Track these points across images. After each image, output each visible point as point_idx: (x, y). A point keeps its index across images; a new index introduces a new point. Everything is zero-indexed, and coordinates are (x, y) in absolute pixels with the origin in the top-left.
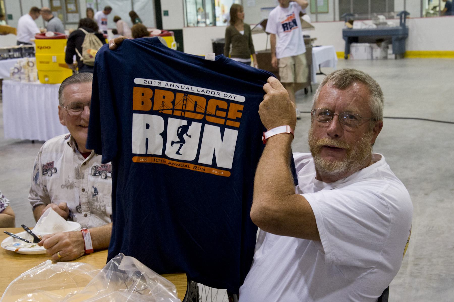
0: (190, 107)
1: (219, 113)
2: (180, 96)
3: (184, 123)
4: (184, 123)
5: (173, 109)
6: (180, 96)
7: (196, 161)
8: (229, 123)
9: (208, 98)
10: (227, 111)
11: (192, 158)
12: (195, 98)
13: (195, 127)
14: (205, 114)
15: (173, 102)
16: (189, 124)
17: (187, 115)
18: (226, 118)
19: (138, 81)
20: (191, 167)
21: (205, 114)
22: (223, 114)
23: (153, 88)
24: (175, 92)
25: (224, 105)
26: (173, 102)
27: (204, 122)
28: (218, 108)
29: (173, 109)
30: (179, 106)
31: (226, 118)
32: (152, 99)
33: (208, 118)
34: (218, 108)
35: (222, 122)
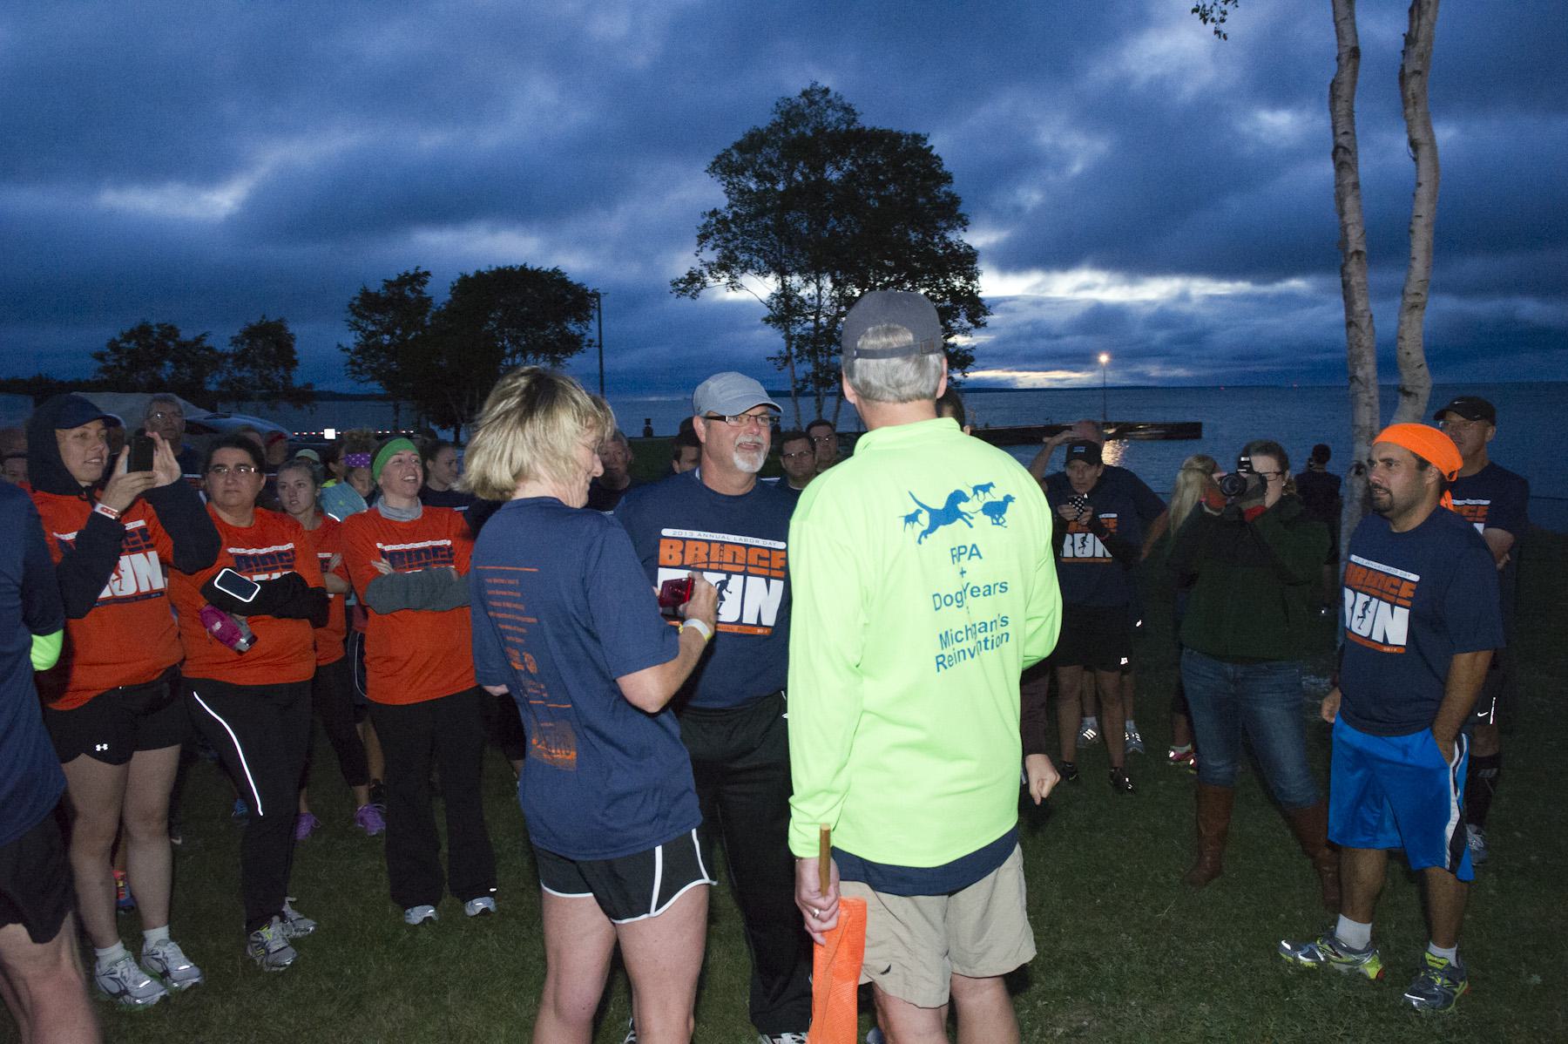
0: (728, 557)
1: (762, 563)
2: (715, 547)
3: (723, 577)
4: (723, 577)
5: (709, 562)
6: (715, 547)
7: (739, 622)
8: (774, 573)
9: (747, 546)
10: (769, 559)
11: (735, 618)
12: (736, 548)
13: (736, 582)
14: (746, 565)
15: (708, 554)
16: (729, 577)
17: (727, 567)
18: (770, 568)
19: (666, 532)
20: (735, 629)
21: (746, 565)
22: (766, 563)
23: (684, 540)
24: (709, 542)
25: (766, 554)
26: (708, 554)
27: (745, 574)
28: (760, 558)
29: (709, 562)
30: (715, 557)
31: (770, 568)
32: (683, 552)
33: (751, 570)
34: (760, 558)
35: (766, 572)
